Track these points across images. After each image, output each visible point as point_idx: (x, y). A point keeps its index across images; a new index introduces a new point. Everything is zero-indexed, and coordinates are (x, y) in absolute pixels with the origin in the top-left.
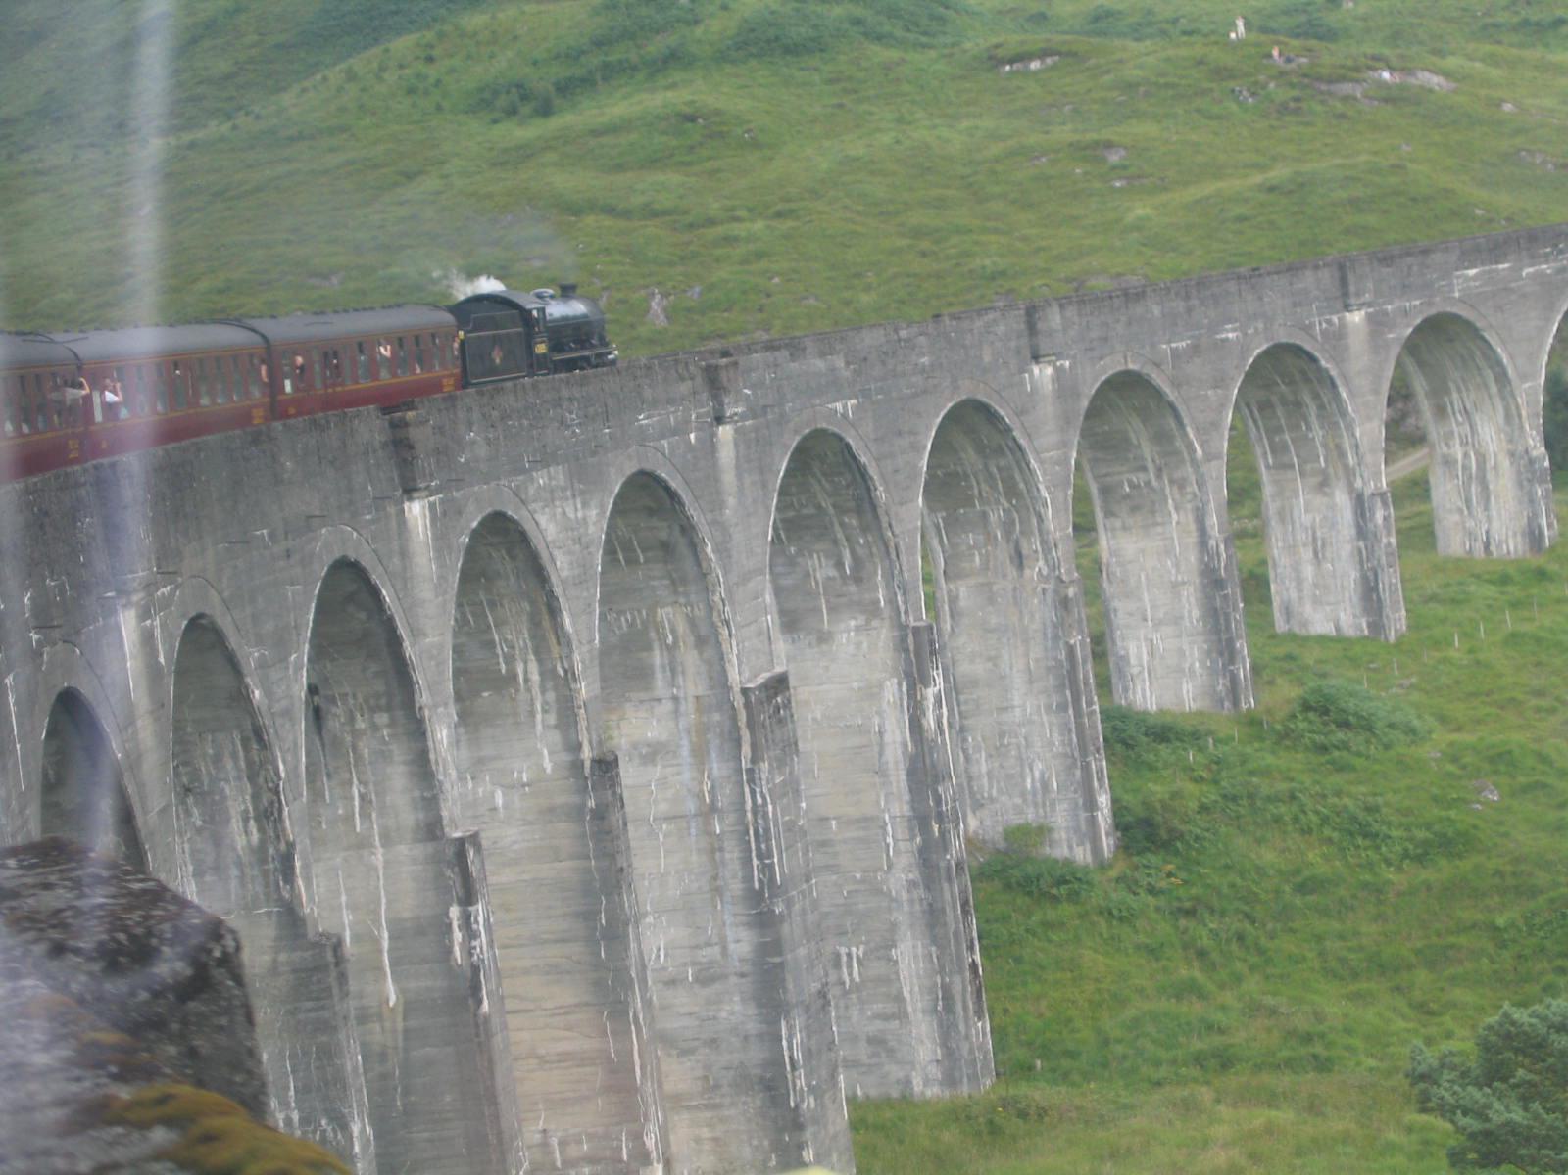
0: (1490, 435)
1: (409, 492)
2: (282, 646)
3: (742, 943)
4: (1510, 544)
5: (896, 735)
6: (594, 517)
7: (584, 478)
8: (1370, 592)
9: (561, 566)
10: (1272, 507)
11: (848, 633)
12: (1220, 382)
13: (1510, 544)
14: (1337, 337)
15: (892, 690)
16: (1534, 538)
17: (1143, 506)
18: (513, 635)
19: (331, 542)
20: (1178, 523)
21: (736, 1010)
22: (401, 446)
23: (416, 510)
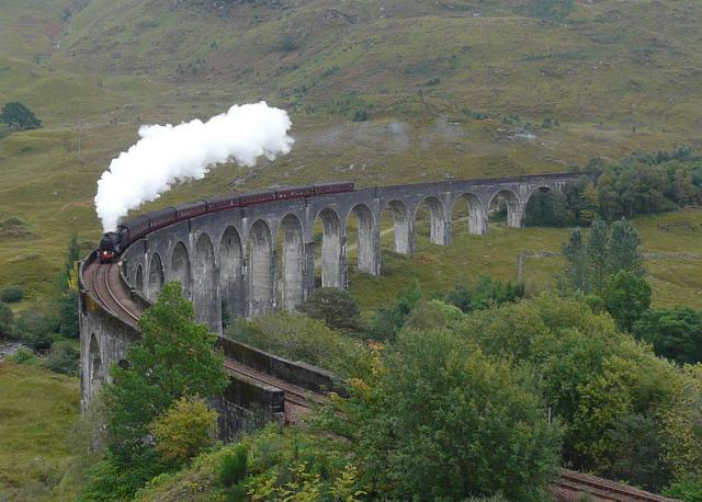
0: (478, 214)
1: (243, 217)
2: (217, 235)
3: (301, 277)
4: (480, 233)
5: (338, 253)
6: (279, 220)
7: (278, 214)
8: (445, 238)
9: (271, 226)
10: (432, 222)
11: (333, 236)
12: (417, 202)
13: (480, 233)
14: (443, 197)
15: (339, 245)
16: (483, 232)
17: (401, 220)
18: (264, 234)
19: (227, 224)
20: (406, 223)
21: (299, 287)
22: (243, 212)
23: (245, 220)
